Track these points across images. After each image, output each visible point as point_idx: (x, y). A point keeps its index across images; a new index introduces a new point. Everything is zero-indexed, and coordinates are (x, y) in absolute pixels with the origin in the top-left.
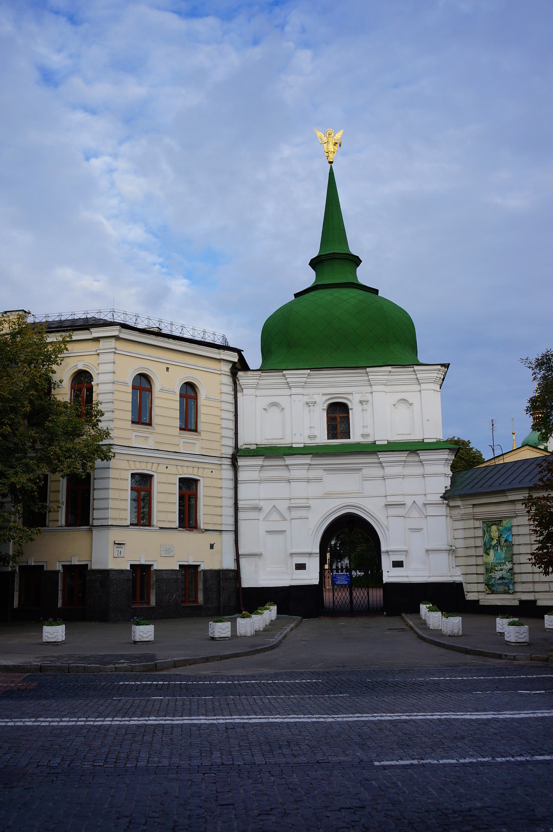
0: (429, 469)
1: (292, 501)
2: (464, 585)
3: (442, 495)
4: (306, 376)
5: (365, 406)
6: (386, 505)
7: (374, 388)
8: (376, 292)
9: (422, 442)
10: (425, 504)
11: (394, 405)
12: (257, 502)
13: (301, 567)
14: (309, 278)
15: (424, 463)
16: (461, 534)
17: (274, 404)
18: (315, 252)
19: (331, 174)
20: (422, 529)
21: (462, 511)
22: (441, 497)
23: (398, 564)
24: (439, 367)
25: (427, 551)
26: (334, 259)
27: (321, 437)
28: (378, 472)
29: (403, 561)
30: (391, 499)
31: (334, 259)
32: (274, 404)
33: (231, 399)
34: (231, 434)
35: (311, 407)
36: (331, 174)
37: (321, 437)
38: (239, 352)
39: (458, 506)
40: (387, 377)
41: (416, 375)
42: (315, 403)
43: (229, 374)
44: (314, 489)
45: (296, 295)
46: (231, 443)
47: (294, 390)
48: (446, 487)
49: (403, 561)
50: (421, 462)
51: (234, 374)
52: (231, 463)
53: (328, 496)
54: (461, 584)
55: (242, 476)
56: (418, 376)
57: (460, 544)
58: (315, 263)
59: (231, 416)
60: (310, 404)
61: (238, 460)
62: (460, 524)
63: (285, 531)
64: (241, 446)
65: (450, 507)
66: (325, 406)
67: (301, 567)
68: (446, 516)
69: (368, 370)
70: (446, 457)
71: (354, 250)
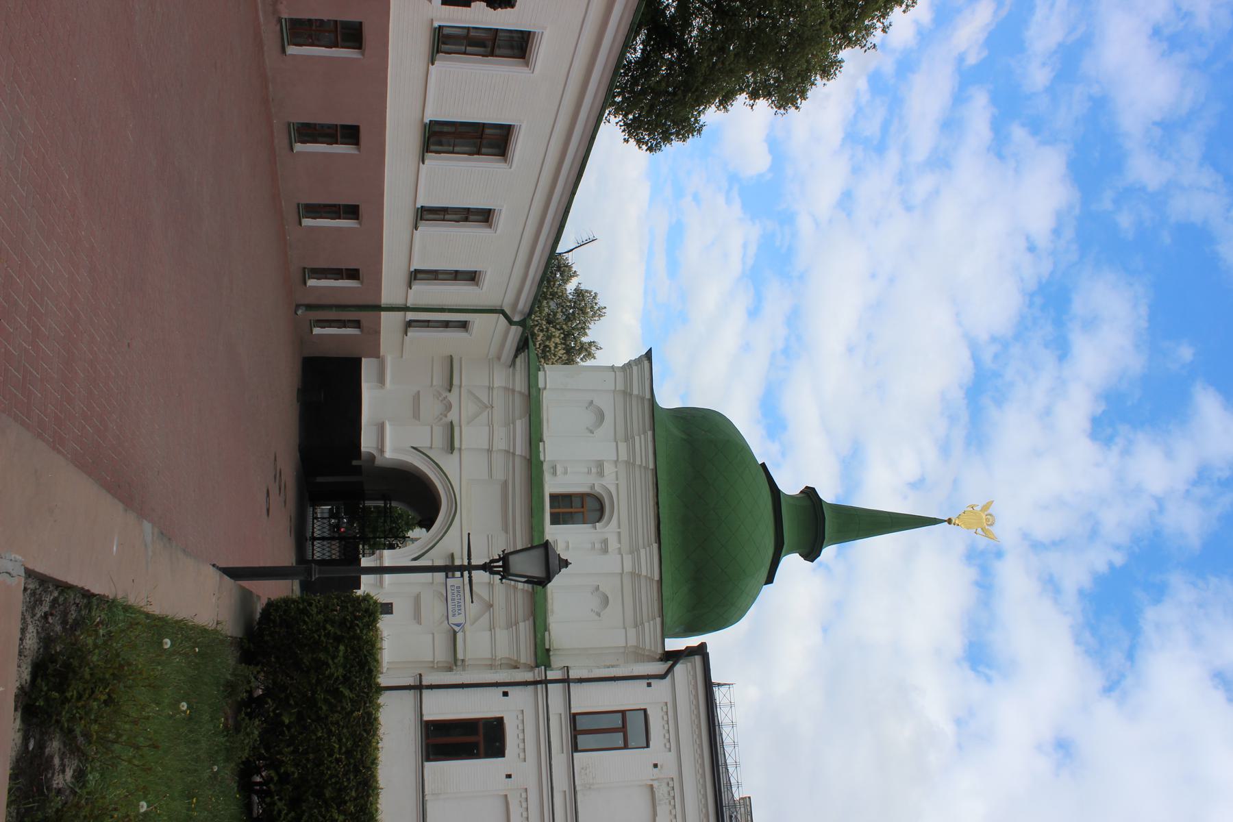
0: (502, 636)
8: (770, 580)
9: (546, 628)
14: (789, 485)
17: (601, 416)
18: (828, 495)
26: (816, 524)
27: (552, 485)
31: (816, 524)
32: (601, 416)
35: (594, 470)
37: (552, 485)
42: (601, 474)
45: (763, 465)
58: (810, 493)
66: (598, 489)
71: (828, 552)
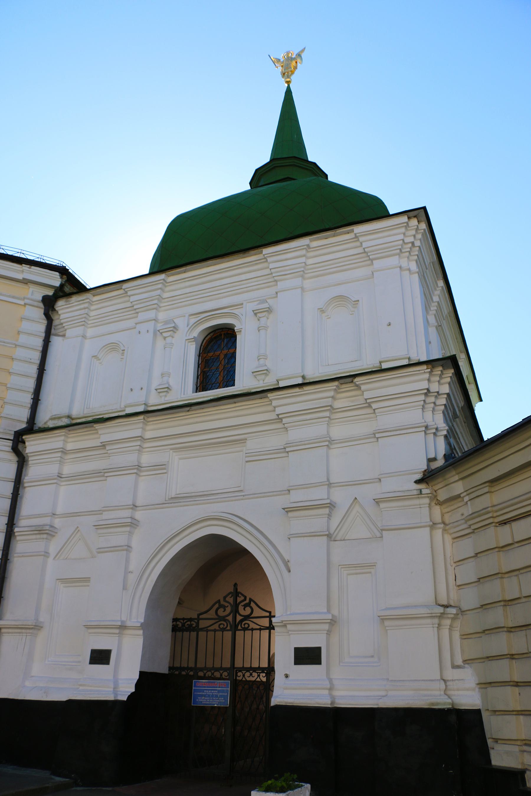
0: (388, 420)
1: (106, 515)
2: (485, 716)
3: (419, 476)
4: (160, 286)
5: (263, 320)
6: (287, 510)
7: (281, 285)
10: (377, 502)
11: (322, 311)
12: (46, 521)
13: (100, 657)
15: (374, 406)
16: (469, 571)
19: (289, 93)
20: (373, 565)
21: (468, 510)
22: (418, 482)
23: (308, 656)
24: (404, 219)
25: (383, 619)
28: (275, 441)
29: (319, 649)
30: (298, 497)
33: (39, 343)
34: (28, 399)
36: (289, 93)
38: (63, 271)
39: (458, 496)
40: (303, 259)
41: (369, 256)
43: (41, 305)
44: (147, 489)
46: (24, 414)
47: (142, 316)
48: (430, 460)
49: (319, 649)
50: (370, 406)
51: (49, 304)
52: (9, 449)
53: (176, 500)
54: (477, 713)
55: (33, 472)
56: (365, 245)
57: (470, 599)
59: (33, 370)
60: (165, 335)
61: (27, 444)
62: (467, 547)
63: (86, 580)
64: (45, 423)
65: (440, 503)
67: (100, 657)
68: (433, 526)
69: (266, 251)
70: (425, 385)
